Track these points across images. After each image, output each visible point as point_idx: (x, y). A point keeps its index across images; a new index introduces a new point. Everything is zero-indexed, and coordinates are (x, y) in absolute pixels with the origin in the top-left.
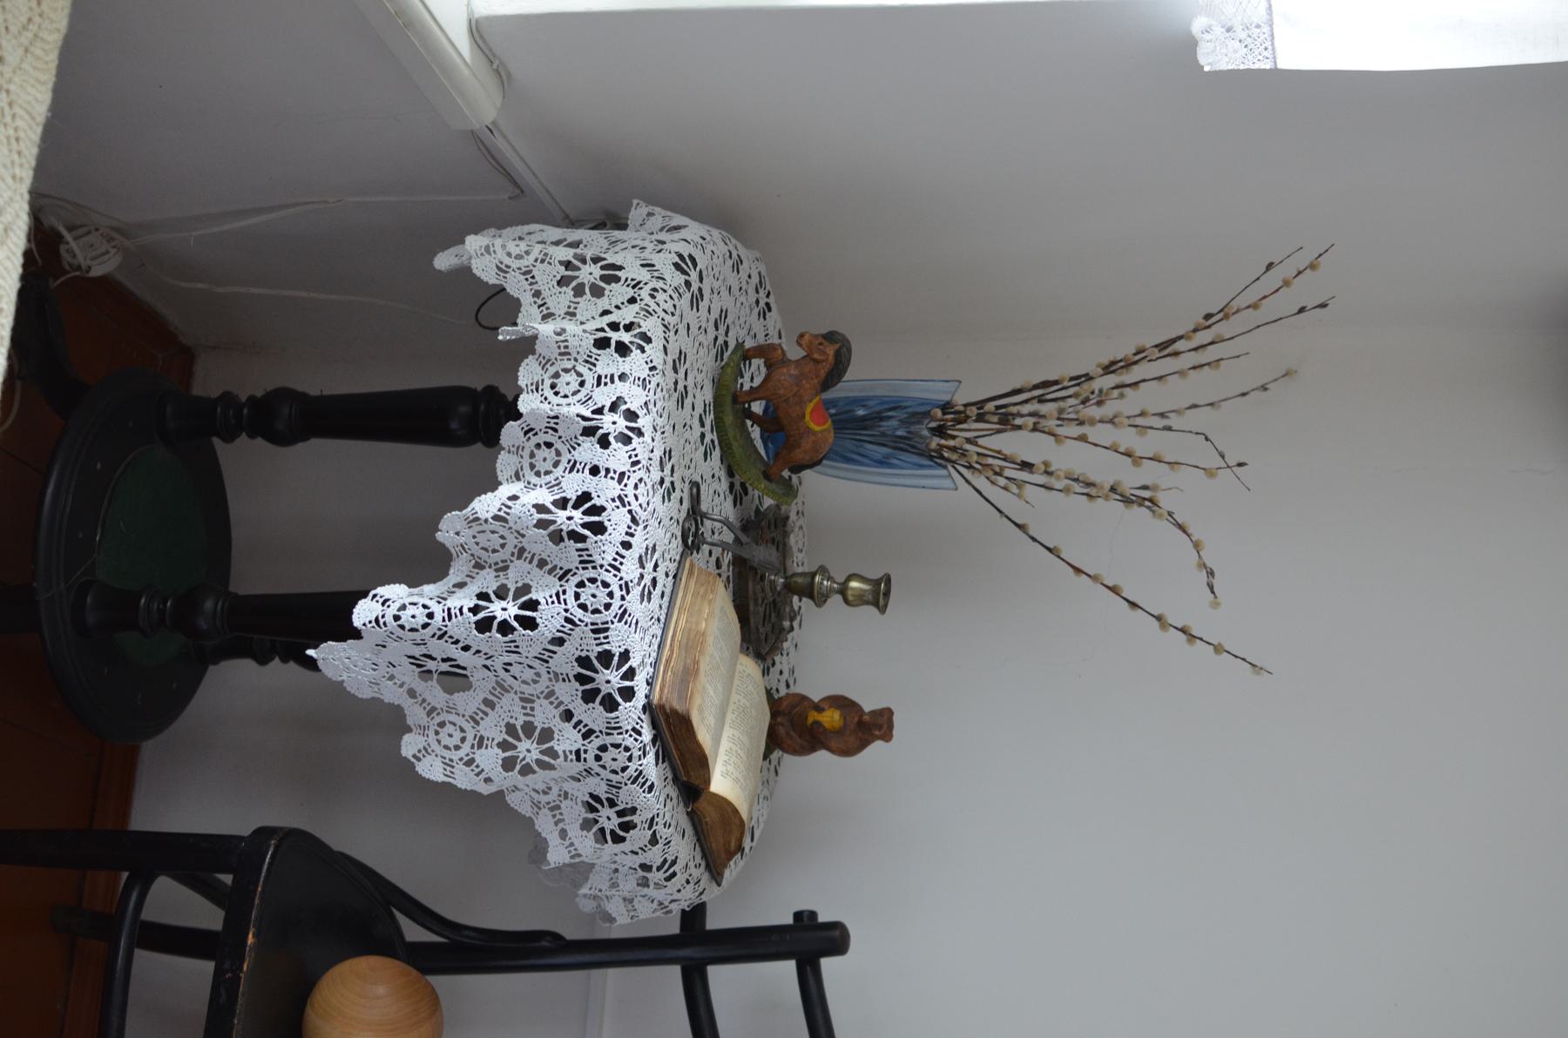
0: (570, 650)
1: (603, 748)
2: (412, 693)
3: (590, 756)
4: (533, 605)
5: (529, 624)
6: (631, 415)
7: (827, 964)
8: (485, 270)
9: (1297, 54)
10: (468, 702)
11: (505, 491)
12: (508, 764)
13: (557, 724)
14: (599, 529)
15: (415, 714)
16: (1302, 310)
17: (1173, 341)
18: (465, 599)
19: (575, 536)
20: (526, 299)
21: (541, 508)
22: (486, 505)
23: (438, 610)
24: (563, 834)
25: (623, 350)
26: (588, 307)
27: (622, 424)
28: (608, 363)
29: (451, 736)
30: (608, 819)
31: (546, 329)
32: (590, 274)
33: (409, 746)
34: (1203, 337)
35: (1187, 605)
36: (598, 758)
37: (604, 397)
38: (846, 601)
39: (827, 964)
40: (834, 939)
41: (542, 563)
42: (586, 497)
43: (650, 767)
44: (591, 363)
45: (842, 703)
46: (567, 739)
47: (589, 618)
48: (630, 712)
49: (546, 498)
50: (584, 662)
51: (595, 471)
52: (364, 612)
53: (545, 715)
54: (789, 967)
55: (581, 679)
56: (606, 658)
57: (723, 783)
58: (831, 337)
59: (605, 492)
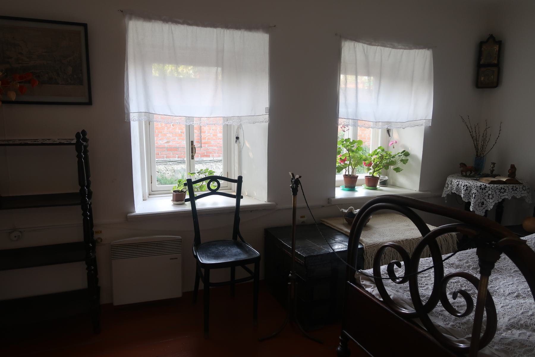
0: (479, 190)
1: (491, 189)
2: (484, 208)
3: (492, 190)
4: (474, 193)
5: (475, 193)
6: (457, 182)
9: (430, 117)
10: (485, 202)
12: (492, 199)
13: (488, 193)
14: (466, 185)
15: (486, 209)
16: (469, 118)
17: (470, 132)
19: (467, 188)
21: (464, 191)
22: (462, 196)
23: (473, 202)
24: (504, 196)
25: (452, 182)
27: (458, 182)
28: (453, 183)
30: (503, 191)
33: (489, 209)
34: (470, 128)
36: (493, 189)
37: (455, 184)
38: (494, 167)
41: (470, 192)
42: (463, 186)
44: (453, 185)
46: (490, 192)
47: (475, 187)
50: (480, 189)
51: (461, 185)
53: (487, 194)
55: (483, 189)
56: (480, 187)
57: (504, 180)
58: (460, 164)
59: (463, 184)
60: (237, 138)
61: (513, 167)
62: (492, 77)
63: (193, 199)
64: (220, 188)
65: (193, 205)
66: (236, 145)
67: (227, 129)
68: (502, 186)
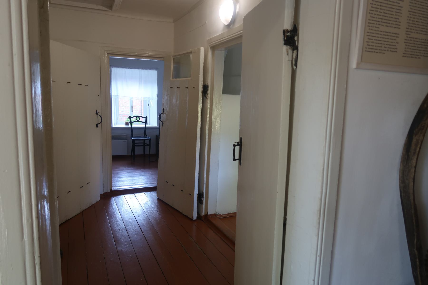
60: (149, 105)
63: (131, 122)
65: (131, 125)
66: (148, 107)
67: (145, 101)
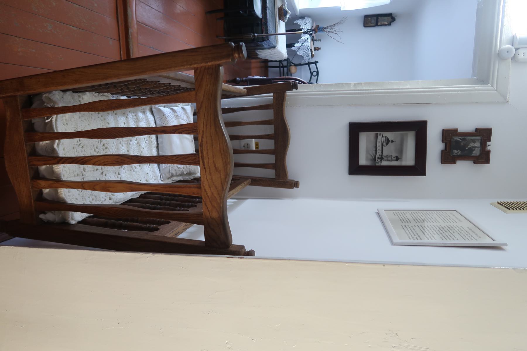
7: (317, 64)
8: (299, 24)
11: (302, 37)
18: (300, 44)
20: (301, 25)
22: (302, 39)
26: (305, 25)
29: (299, 52)
31: (303, 28)
32: (305, 23)
35: (339, 40)
39: (317, 64)
40: (317, 62)
43: (310, 53)
45: (318, 47)
46: (306, 51)
48: (310, 50)
49: (305, 38)
52: (295, 45)
53: (305, 50)
54: (315, 64)
57: (313, 53)
61: (319, 49)
62: (370, 23)
64: (315, 70)
68: (310, 54)
